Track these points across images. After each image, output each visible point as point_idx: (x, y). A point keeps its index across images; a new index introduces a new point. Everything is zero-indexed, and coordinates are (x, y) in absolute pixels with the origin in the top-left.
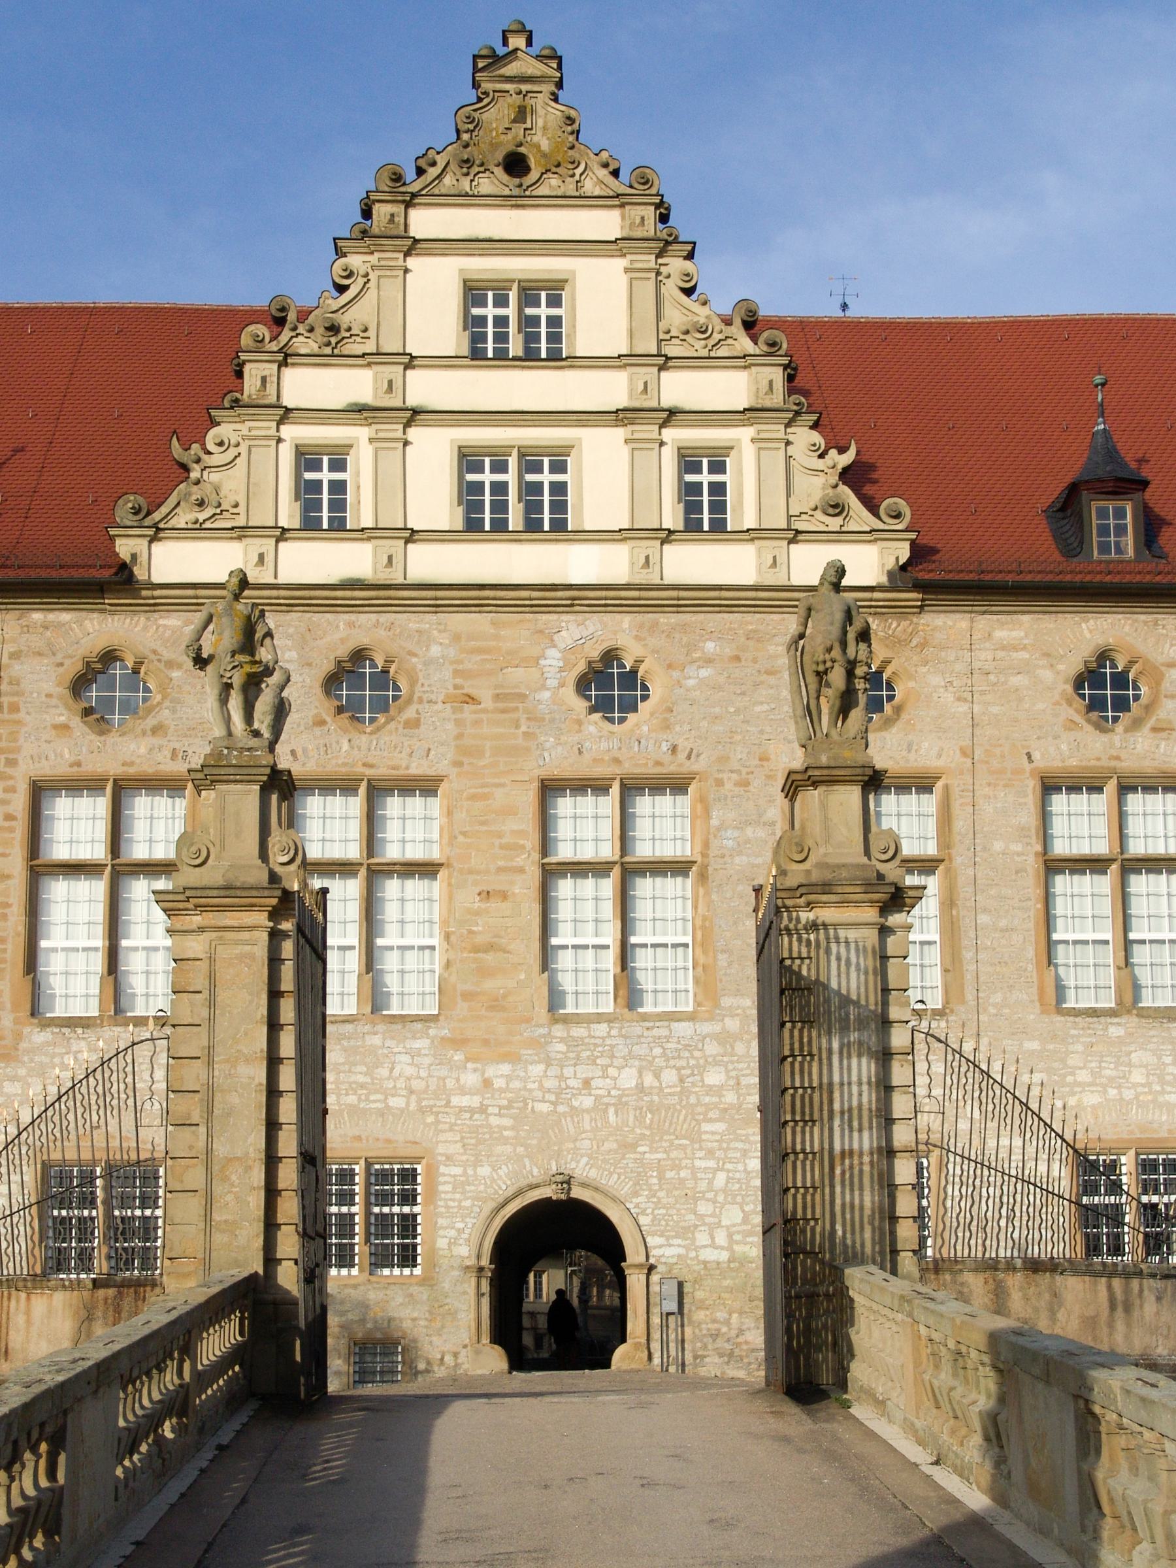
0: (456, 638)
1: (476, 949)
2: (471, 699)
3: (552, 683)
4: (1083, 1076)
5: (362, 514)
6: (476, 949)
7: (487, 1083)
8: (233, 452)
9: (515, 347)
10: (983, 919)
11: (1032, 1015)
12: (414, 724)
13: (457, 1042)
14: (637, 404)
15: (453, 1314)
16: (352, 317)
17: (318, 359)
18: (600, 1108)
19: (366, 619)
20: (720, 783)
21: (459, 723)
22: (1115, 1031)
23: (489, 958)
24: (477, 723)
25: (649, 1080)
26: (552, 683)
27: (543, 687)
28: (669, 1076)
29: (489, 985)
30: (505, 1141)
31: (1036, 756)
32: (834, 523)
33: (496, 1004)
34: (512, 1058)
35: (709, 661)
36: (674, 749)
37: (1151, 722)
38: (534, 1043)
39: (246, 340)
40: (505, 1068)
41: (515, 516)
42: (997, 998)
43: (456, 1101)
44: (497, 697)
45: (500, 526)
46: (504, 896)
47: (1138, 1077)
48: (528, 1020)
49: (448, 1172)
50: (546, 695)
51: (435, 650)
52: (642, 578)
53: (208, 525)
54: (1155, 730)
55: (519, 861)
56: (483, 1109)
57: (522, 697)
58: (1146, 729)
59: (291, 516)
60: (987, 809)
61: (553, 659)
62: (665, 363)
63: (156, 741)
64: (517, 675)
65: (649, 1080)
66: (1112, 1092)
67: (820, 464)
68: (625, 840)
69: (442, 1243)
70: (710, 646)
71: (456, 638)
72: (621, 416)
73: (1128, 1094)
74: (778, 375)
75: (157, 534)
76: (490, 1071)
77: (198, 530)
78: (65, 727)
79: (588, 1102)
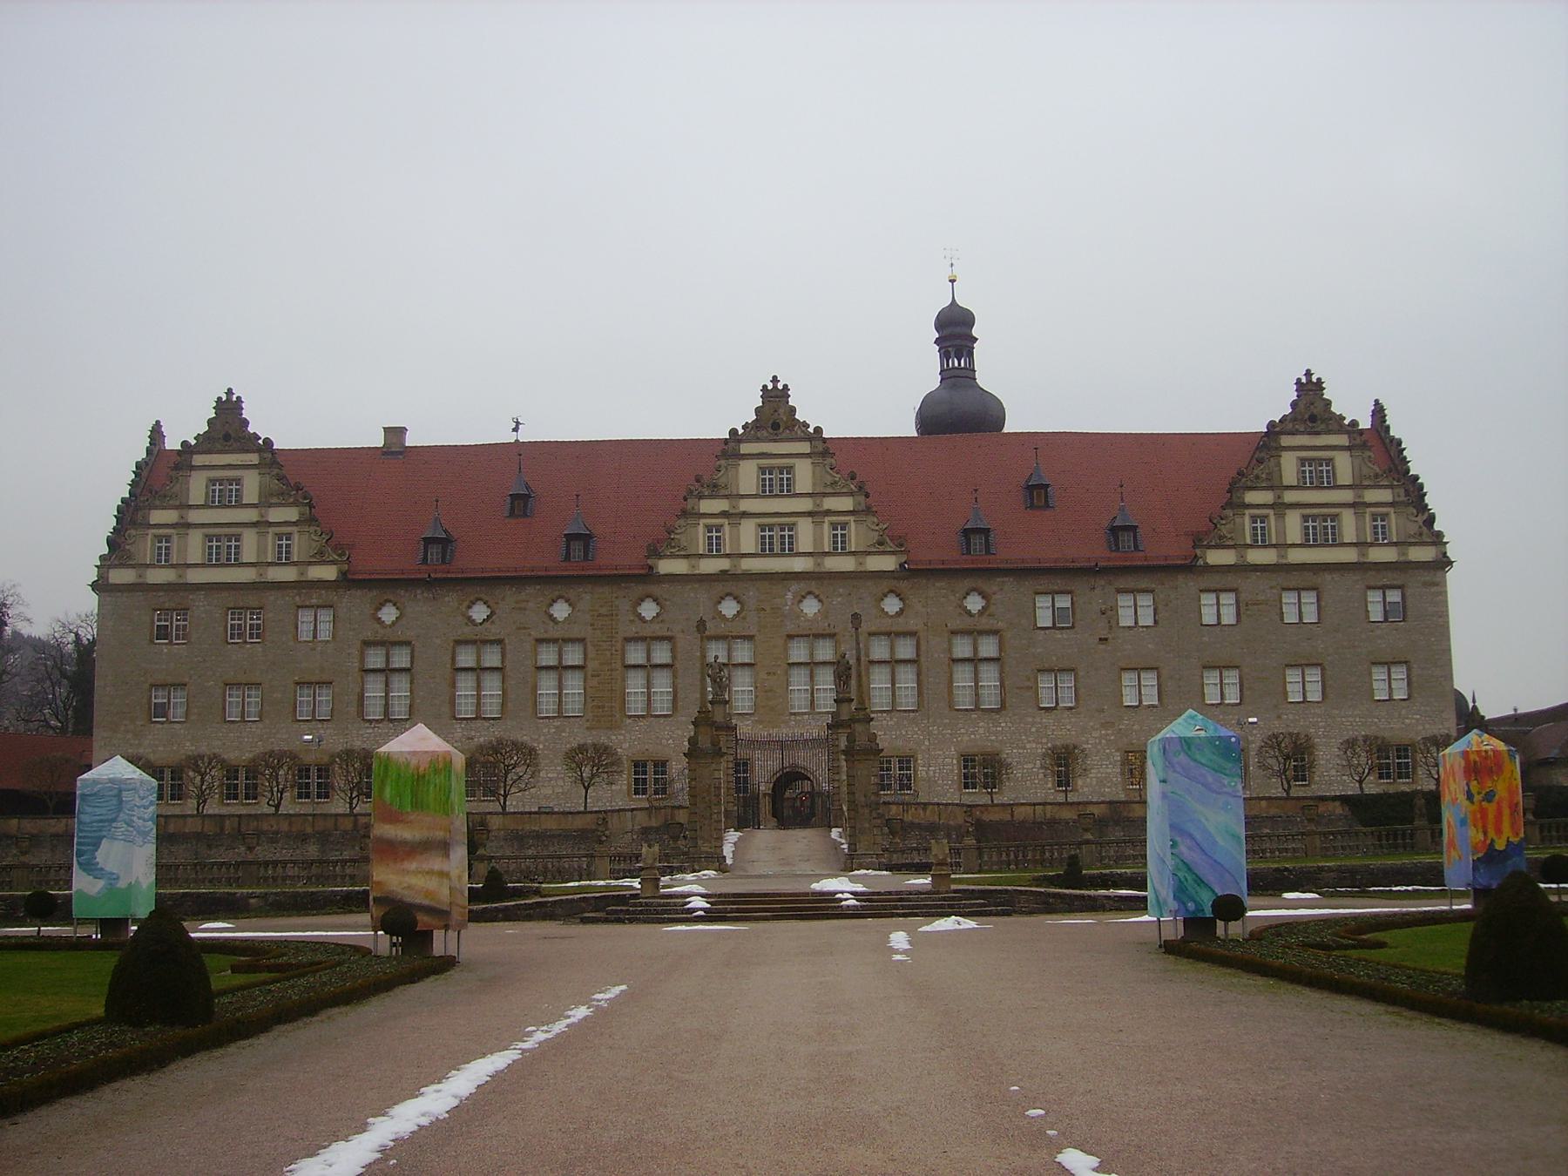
1: (766, 692)
3: (789, 603)
6: (766, 692)
8: (684, 529)
12: (744, 618)
16: (722, 481)
17: (711, 497)
23: (769, 694)
26: (789, 603)
27: (787, 605)
31: (949, 625)
32: (882, 548)
35: (841, 595)
36: (829, 625)
47: (981, 731)
48: (782, 715)
50: (788, 607)
53: (677, 553)
54: (989, 615)
55: (779, 663)
58: (985, 616)
59: (704, 550)
61: (790, 596)
62: (825, 495)
63: (661, 625)
66: (973, 736)
70: (841, 590)
78: (632, 621)
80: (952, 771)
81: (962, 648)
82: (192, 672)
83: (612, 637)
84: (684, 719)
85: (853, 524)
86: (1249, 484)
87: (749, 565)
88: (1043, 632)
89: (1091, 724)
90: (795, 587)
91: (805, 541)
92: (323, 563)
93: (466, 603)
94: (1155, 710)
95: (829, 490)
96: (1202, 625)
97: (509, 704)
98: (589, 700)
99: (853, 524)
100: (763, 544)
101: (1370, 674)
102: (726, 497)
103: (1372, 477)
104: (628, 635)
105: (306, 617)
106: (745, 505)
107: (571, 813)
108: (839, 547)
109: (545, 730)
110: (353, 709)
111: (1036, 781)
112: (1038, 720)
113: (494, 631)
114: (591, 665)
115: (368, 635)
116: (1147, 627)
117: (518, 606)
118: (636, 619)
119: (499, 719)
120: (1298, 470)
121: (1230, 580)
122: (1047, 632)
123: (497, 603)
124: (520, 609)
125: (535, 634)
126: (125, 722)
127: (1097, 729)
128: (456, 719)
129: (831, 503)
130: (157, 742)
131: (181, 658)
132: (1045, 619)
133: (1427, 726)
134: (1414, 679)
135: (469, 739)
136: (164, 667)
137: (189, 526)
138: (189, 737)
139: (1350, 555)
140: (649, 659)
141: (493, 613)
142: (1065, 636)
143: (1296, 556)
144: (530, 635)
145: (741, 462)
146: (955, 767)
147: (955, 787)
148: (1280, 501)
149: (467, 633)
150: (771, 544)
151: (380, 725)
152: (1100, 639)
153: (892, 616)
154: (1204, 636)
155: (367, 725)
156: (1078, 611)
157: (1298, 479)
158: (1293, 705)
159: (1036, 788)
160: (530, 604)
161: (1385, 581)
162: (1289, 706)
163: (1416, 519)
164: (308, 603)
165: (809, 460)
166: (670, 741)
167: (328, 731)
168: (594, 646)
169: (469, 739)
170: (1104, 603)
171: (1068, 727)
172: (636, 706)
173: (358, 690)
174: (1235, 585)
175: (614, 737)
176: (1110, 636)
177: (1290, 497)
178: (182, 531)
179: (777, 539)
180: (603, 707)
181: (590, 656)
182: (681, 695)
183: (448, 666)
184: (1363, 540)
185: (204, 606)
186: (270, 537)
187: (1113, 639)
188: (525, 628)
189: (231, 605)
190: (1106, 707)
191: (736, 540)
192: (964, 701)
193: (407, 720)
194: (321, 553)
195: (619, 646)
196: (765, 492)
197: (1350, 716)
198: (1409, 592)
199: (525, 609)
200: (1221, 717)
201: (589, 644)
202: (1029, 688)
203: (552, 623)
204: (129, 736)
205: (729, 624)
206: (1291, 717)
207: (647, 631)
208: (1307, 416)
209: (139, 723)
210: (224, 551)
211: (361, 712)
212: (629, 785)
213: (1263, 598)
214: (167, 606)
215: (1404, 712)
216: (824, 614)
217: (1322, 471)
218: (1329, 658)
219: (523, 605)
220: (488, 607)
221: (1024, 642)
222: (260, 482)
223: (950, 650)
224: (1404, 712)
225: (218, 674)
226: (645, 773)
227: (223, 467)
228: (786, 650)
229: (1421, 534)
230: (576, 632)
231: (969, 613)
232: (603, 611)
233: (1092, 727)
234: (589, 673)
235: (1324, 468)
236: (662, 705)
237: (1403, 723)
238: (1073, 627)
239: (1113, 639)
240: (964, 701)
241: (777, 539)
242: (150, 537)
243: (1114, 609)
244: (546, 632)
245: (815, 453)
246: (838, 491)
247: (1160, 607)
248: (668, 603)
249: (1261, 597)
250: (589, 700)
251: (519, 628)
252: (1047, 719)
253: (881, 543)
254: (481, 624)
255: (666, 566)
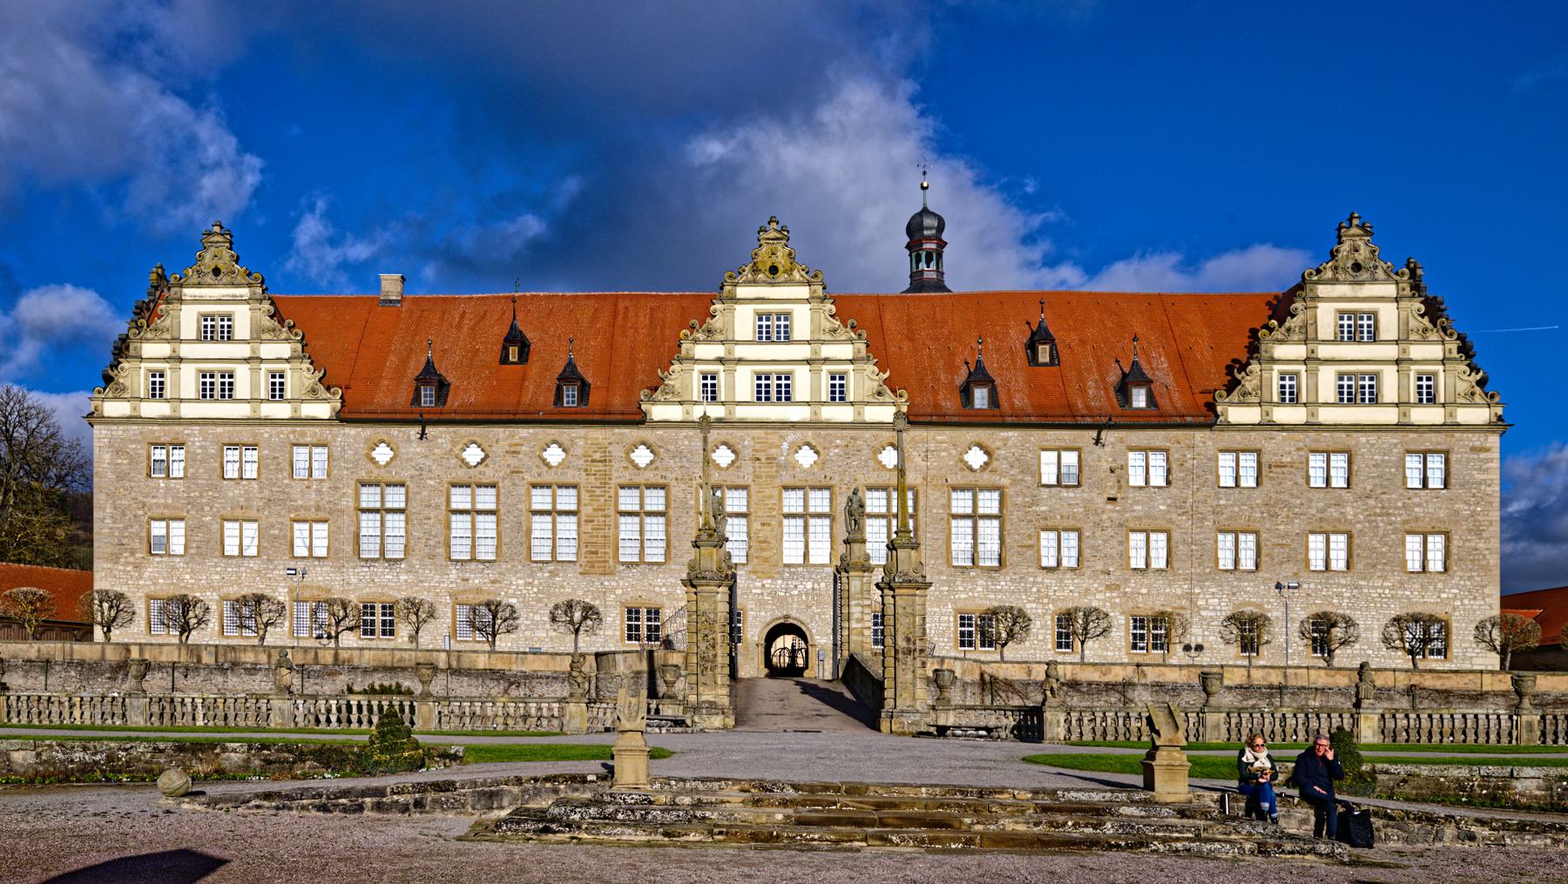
0: (753, 438)
1: (760, 542)
2: (758, 459)
4: (961, 588)
5: (722, 396)
6: (760, 542)
7: (763, 586)
9: (774, 338)
10: (929, 535)
11: (944, 568)
12: (739, 467)
13: (755, 572)
14: (814, 357)
15: (753, 659)
17: (706, 342)
18: (800, 595)
19: (724, 432)
20: (840, 488)
21: (754, 467)
22: (972, 574)
23: (764, 545)
24: (760, 467)
25: (816, 586)
28: (823, 585)
29: (765, 554)
30: (769, 604)
33: (766, 560)
34: (772, 578)
35: (837, 447)
37: (990, 469)
38: (779, 573)
39: (682, 336)
40: (770, 581)
41: (774, 396)
42: (933, 562)
43: (754, 591)
44: (767, 459)
45: (767, 399)
46: (769, 525)
47: (980, 589)
49: (752, 613)
51: (746, 443)
52: (815, 418)
55: (774, 513)
56: (762, 594)
57: (775, 459)
58: (987, 471)
60: (931, 497)
61: (785, 446)
62: (824, 342)
64: (773, 451)
65: (816, 586)
67: (877, 378)
68: (806, 506)
69: (749, 636)
70: (838, 442)
71: (753, 438)
72: (808, 362)
73: (976, 595)
74: (863, 347)
75: (655, 402)
76: (765, 582)
77: (667, 402)
78: (626, 468)
79: (796, 592)
80: (948, 628)
81: (961, 503)
82: (189, 507)
83: (605, 483)
84: (678, 567)
85: (852, 374)
86: (1280, 337)
87: (742, 413)
88: (1047, 490)
89: (1096, 585)
90: (792, 436)
91: (801, 390)
92: (317, 400)
93: (460, 446)
94: (1164, 574)
95: (828, 337)
96: (1219, 487)
97: (504, 548)
98: (583, 546)
99: (852, 373)
100: (759, 392)
101: (1403, 543)
102: (722, 342)
103: (1420, 332)
104: (622, 481)
105: (301, 454)
106: (740, 351)
107: (560, 654)
108: (838, 394)
109: (539, 574)
110: (349, 548)
111: (1036, 642)
112: (1039, 579)
113: (489, 474)
114: (586, 511)
115: (363, 475)
116: (1159, 488)
117: (513, 449)
118: (630, 466)
119: (494, 561)
120: (1336, 323)
121: (1256, 439)
122: (1053, 490)
123: (490, 446)
124: (514, 452)
125: (528, 478)
126: (125, 555)
127: (1101, 592)
128: (451, 561)
129: (827, 351)
130: (156, 575)
131: (179, 493)
132: (1049, 477)
133: (1466, 602)
134: (1454, 550)
135: (464, 580)
136: (162, 501)
137: (181, 360)
138: (189, 570)
139: (1390, 416)
140: (642, 505)
141: (487, 456)
142: (1071, 495)
143: (1326, 415)
144: (523, 479)
145: (736, 306)
146: (952, 625)
147: (952, 644)
148: (1314, 356)
149: (461, 474)
150: (767, 392)
151: (377, 564)
152: (1109, 499)
153: (890, 470)
154: (1220, 499)
155: (363, 564)
156: (1086, 469)
157: (1335, 333)
158: (1315, 574)
159: (1035, 649)
160: (523, 448)
161: (1428, 446)
162: (1311, 575)
163: (1469, 378)
164: (302, 441)
165: (808, 306)
166: (664, 589)
167: (325, 569)
168: (587, 491)
169: (464, 580)
170: (1115, 461)
171: (1071, 588)
172: (628, 553)
173: (353, 529)
174: (1258, 446)
175: (606, 583)
176: (1119, 496)
177: (1324, 351)
178: (176, 365)
179: (774, 389)
180: (596, 553)
181: (583, 502)
182: (674, 543)
183: (443, 508)
184: (1404, 399)
185: (199, 441)
186: (263, 373)
187: (1123, 499)
188: (517, 472)
189: (226, 440)
190: (1111, 569)
191: (731, 387)
192: (961, 556)
193: (402, 560)
194: (314, 391)
195: (612, 492)
196: (764, 336)
197: (1378, 587)
198: (1453, 457)
199: (519, 453)
200: (1235, 583)
201: (582, 489)
202: (1031, 547)
203: (545, 469)
204: (129, 568)
205: (723, 473)
206: (1312, 586)
207: (641, 479)
208: (1350, 264)
209: (138, 555)
210: (218, 387)
211: (358, 552)
212: (622, 630)
213: (1289, 460)
214: (162, 440)
215: (1440, 585)
216: (821, 464)
217: (1362, 326)
218: (1359, 526)
219: (518, 448)
220: (482, 450)
221: (1027, 499)
222: (251, 318)
223: (949, 506)
224: (1440, 585)
225: (215, 510)
226: (637, 619)
227: (219, 301)
228: (780, 499)
229: (1473, 394)
230: (569, 479)
231: (971, 469)
232: (597, 456)
233: (1096, 589)
234: (584, 518)
235: (1365, 322)
236: (655, 553)
237: (1439, 597)
238: (1079, 485)
239: (1123, 499)
240: (961, 556)
241: (774, 389)
242: (142, 371)
243: (1124, 467)
244: (539, 475)
245: (813, 298)
246: (837, 338)
247: (1174, 466)
248: (662, 450)
249: (1287, 459)
250: (583, 546)
251: (513, 472)
252: (1049, 580)
253: (879, 394)
254: (475, 467)
255: (658, 412)
